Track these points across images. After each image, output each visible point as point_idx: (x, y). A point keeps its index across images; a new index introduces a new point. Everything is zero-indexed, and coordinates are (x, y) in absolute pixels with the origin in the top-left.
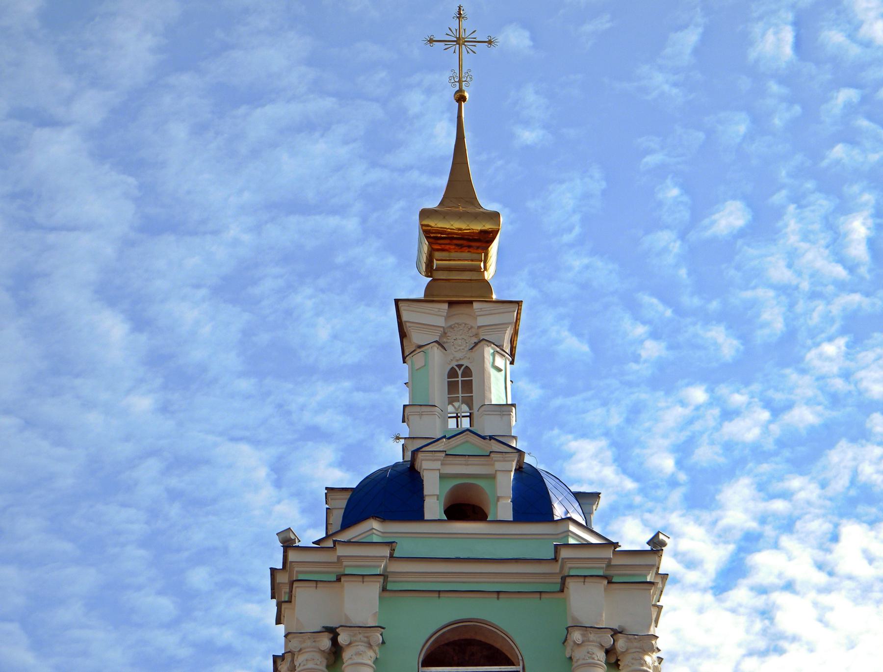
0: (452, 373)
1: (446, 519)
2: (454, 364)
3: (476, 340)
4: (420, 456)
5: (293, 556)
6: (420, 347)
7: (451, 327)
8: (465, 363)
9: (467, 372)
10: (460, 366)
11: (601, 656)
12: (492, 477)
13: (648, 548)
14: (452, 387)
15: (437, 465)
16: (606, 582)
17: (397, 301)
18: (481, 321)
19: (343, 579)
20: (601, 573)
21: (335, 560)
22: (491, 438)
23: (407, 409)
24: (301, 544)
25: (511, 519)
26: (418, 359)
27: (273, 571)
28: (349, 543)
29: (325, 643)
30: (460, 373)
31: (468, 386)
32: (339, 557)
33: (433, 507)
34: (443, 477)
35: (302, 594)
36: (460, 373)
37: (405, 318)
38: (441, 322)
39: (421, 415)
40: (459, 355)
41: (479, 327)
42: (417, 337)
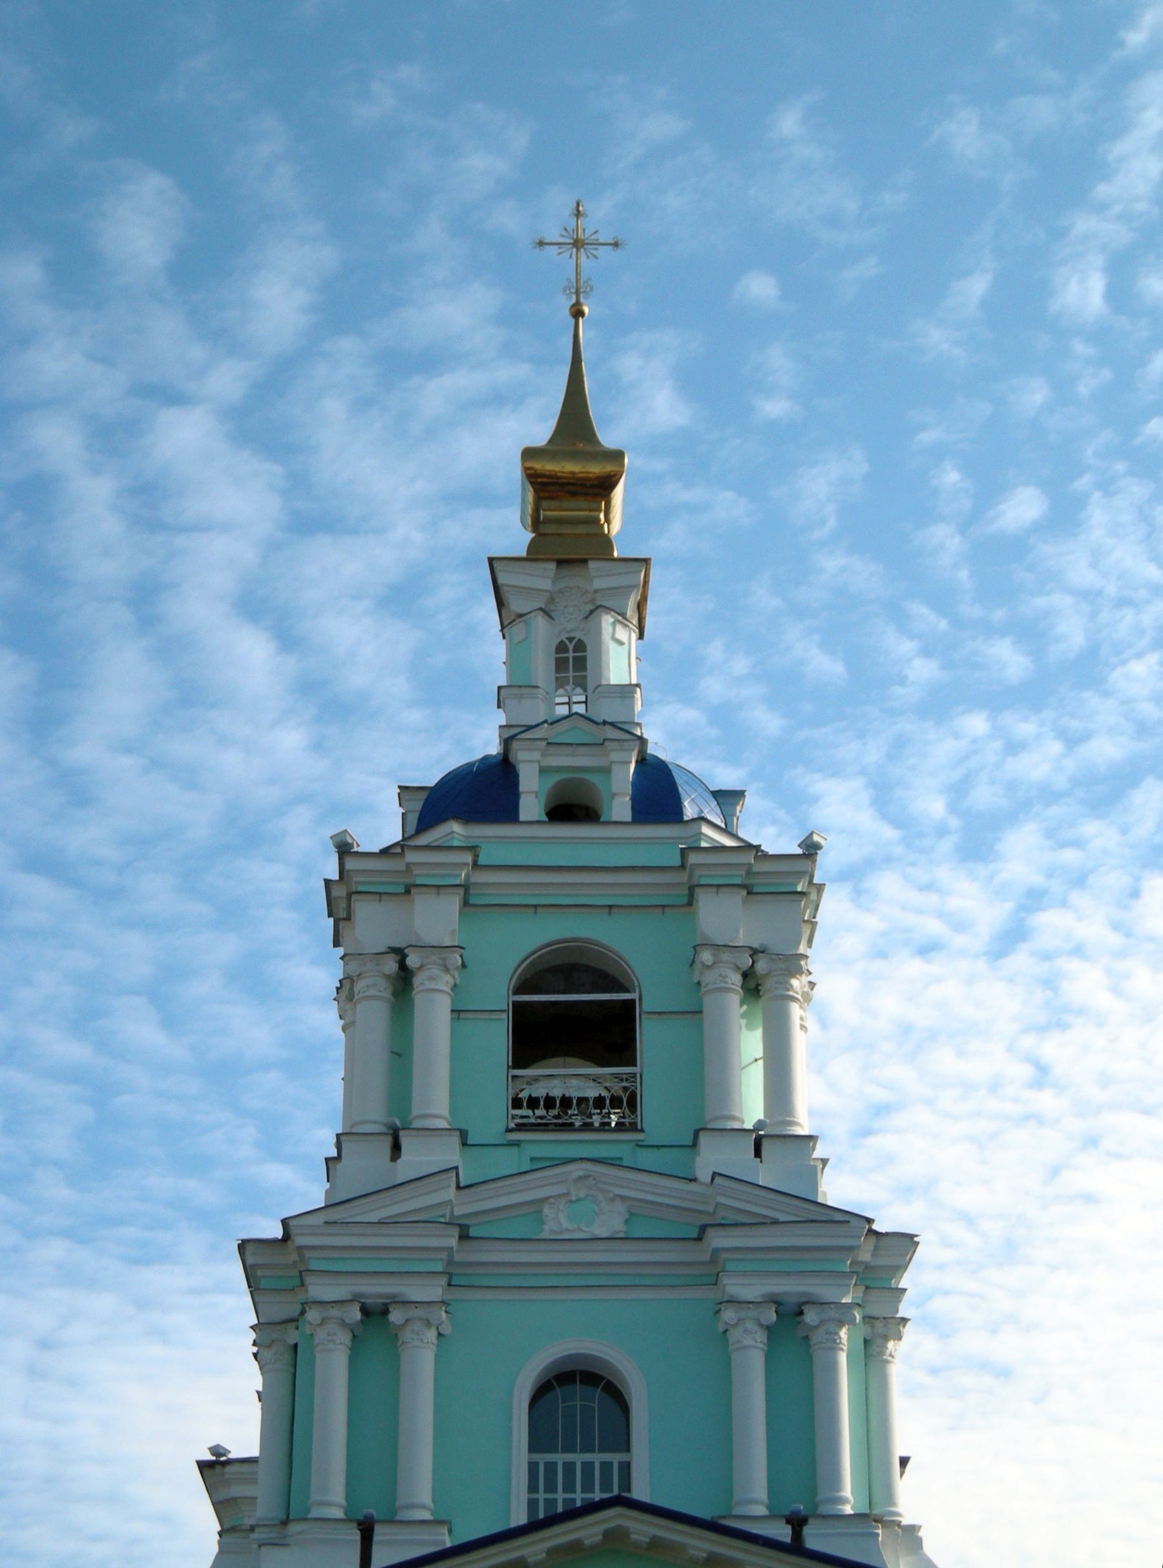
0: (561, 648)
2: (564, 637)
3: (592, 607)
4: (515, 745)
5: (351, 864)
6: (521, 616)
7: (560, 591)
8: (578, 635)
9: (580, 646)
10: (571, 639)
11: (736, 979)
12: (606, 771)
13: (800, 851)
14: (561, 665)
15: (536, 755)
16: (744, 892)
17: (491, 560)
18: (598, 584)
19: (413, 891)
20: (738, 881)
21: (403, 868)
22: (605, 723)
23: (503, 692)
24: (360, 850)
25: (629, 818)
26: (518, 630)
27: (328, 882)
29: (391, 966)
30: (571, 647)
32: (408, 865)
33: (531, 806)
34: (543, 771)
35: (363, 910)
36: (571, 647)
37: (502, 580)
38: (546, 584)
39: (520, 698)
40: (570, 626)
41: (596, 591)
42: (516, 605)
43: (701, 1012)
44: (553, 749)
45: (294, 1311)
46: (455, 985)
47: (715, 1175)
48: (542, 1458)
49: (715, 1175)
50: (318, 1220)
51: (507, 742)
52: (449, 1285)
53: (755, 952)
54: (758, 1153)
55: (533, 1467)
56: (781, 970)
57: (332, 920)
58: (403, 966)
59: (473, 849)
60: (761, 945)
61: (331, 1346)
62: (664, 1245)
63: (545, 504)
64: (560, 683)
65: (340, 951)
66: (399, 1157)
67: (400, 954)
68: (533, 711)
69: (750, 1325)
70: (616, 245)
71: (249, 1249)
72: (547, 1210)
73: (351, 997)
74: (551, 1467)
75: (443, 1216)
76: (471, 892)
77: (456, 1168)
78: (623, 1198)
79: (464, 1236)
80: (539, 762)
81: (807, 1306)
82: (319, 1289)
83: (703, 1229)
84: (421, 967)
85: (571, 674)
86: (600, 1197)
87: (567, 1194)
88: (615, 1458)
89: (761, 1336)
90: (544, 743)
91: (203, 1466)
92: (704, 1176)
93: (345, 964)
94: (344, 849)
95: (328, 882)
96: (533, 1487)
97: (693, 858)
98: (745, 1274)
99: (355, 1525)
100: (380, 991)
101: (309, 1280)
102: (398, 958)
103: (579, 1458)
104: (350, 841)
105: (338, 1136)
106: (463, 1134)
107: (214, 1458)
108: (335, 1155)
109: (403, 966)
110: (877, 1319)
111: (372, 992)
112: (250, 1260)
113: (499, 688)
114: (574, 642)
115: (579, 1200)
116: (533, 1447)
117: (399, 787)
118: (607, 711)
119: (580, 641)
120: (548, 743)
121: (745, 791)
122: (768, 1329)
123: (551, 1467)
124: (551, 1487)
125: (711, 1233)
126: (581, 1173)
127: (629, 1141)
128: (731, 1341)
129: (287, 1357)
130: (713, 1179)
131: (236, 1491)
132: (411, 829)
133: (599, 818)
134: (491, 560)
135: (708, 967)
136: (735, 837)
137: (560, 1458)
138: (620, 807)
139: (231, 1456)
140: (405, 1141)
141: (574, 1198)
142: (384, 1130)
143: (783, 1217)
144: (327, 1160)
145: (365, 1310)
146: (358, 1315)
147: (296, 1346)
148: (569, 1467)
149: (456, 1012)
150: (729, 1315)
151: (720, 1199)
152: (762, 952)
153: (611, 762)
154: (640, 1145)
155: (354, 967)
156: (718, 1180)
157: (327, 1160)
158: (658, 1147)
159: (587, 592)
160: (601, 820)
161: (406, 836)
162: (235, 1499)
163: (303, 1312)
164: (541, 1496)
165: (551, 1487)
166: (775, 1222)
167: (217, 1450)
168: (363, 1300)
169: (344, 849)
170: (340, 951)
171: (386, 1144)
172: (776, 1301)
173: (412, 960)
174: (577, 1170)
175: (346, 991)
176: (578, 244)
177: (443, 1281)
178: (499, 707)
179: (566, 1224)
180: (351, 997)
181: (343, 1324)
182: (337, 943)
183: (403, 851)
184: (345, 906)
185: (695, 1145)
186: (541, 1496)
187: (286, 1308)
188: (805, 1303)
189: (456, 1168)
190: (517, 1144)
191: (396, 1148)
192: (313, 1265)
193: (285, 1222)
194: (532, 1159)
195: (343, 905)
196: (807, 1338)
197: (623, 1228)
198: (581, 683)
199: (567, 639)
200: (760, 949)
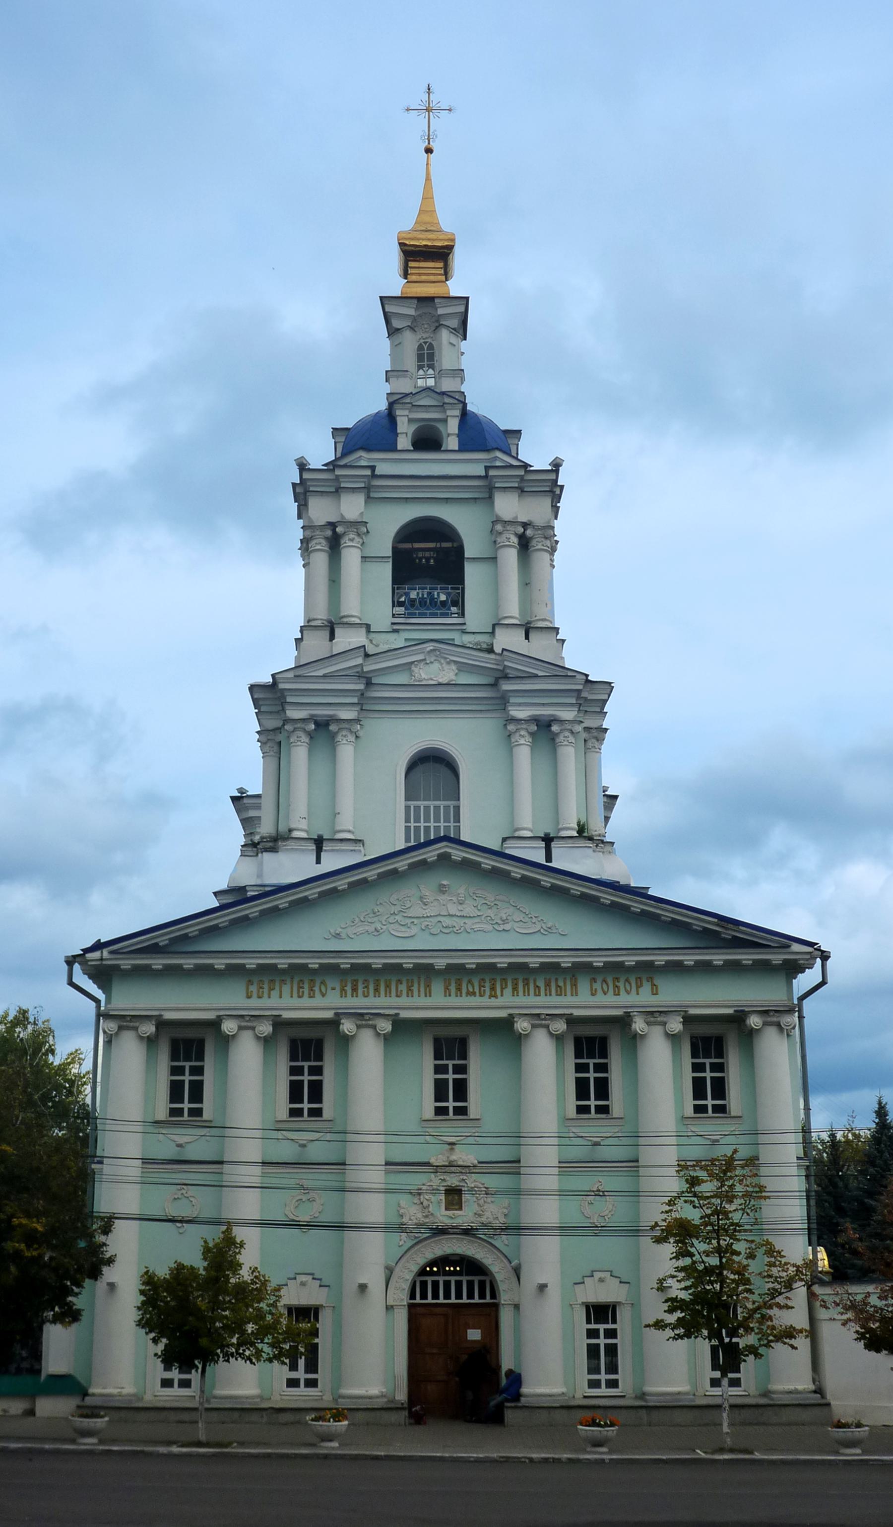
0: (420, 347)
1: (412, 449)
2: (422, 341)
3: (437, 325)
4: (396, 406)
5: (306, 476)
6: (399, 329)
8: (429, 340)
9: (431, 347)
10: (425, 343)
12: (445, 421)
14: (420, 358)
15: (406, 412)
17: (381, 298)
18: (440, 311)
19: (339, 490)
22: (443, 393)
23: (388, 373)
24: (311, 467)
25: (457, 448)
26: (398, 338)
27: (294, 485)
28: (345, 466)
29: (329, 533)
31: (431, 357)
32: (337, 476)
33: (404, 442)
34: (410, 421)
37: (387, 310)
38: (412, 312)
39: (398, 377)
40: (425, 336)
41: (439, 315)
43: (496, 558)
44: (415, 409)
45: (279, 724)
46: (363, 542)
47: (503, 650)
48: (412, 804)
49: (503, 650)
50: (290, 675)
51: (391, 405)
52: (362, 709)
53: (525, 525)
54: (527, 637)
55: (407, 808)
56: (539, 534)
57: (297, 504)
58: (334, 531)
59: (373, 468)
60: (529, 521)
61: (299, 743)
62: (476, 688)
63: (411, 264)
64: (420, 367)
65: (301, 523)
66: (334, 639)
67: (332, 525)
68: (404, 386)
69: (523, 733)
70: (450, 110)
71: (255, 689)
72: (413, 668)
73: (307, 549)
74: (417, 808)
75: (358, 672)
76: (371, 490)
77: (364, 646)
78: (454, 661)
79: (369, 683)
80: (408, 416)
81: (554, 722)
82: (293, 713)
83: (497, 679)
84: (345, 533)
85: (426, 363)
86: (442, 661)
87: (425, 660)
88: (451, 803)
89: (529, 739)
90: (410, 405)
91: (234, 799)
92: (498, 649)
93: (304, 531)
94: (302, 466)
95: (294, 485)
96: (407, 820)
97: (492, 473)
98: (520, 704)
99: (313, 841)
100: (322, 546)
101: (287, 707)
102: (332, 528)
103: (432, 804)
104: (305, 462)
105: (301, 627)
106: (368, 627)
107: (239, 795)
108: (300, 637)
109: (334, 531)
110: (591, 728)
111: (318, 547)
112: (255, 697)
113: (387, 372)
114: (428, 344)
115: (432, 663)
116: (407, 798)
117: (332, 428)
118: (447, 385)
119: (430, 343)
120: (413, 405)
121: (521, 431)
122: (532, 734)
123: (417, 808)
124: (417, 820)
125: (501, 682)
126: (431, 648)
127: (458, 630)
128: (513, 740)
129: (276, 748)
130: (502, 652)
131: (252, 813)
132: (339, 455)
133: (441, 446)
134: (381, 298)
135: (500, 533)
136: (517, 459)
137: (422, 804)
138: (452, 443)
139: (248, 794)
140: (338, 631)
141: (428, 662)
142: (326, 623)
143: (540, 673)
144: (296, 640)
145: (317, 724)
146: (313, 727)
147: (280, 742)
148: (427, 808)
149: (364, 558)
150: (511, 727)
151: (506, 663)
152: (529, 525)
153: (447, 416)
154: (464, 632)
155: (309, 533)
156: (505, 653)
157: (296, 640)
158: (474, 633)
159: (434, 316)
160: (442, 449)
161: (337, 457)
162: (251, 818)
163: (284, 725)
164: (412, 825)
165: (417, 820)
166: (536, 676)
167: (241, 791)
168: (315, 718)
169: (302, 466)
170: (301, 523)
171: (326, 634)
172: (536, 720)
173: (339, 530)
174: (430, 646)
175: (306, 545)
176: (429, 110)
177: (358, 708)
178: (386, 381)
179: (424, 676)
180: (307, 549)
181: (304, 730)
182: (299, 517)
183: (334, 468)
184: (303, 497)
185: (494, 626)
186: (412, 825)
187: (276, 723)
188: (552, 720)
189: (364, 646)
190: (396, 631)
191: (332, 637)
192: (289, 699)
193: (273, 676)
194: (406, 640)
195: (302, 497)
196: (553, 739)
197: (454, 677)
198: (432, 366)
199: (424, 342)
200: (528, 523)
